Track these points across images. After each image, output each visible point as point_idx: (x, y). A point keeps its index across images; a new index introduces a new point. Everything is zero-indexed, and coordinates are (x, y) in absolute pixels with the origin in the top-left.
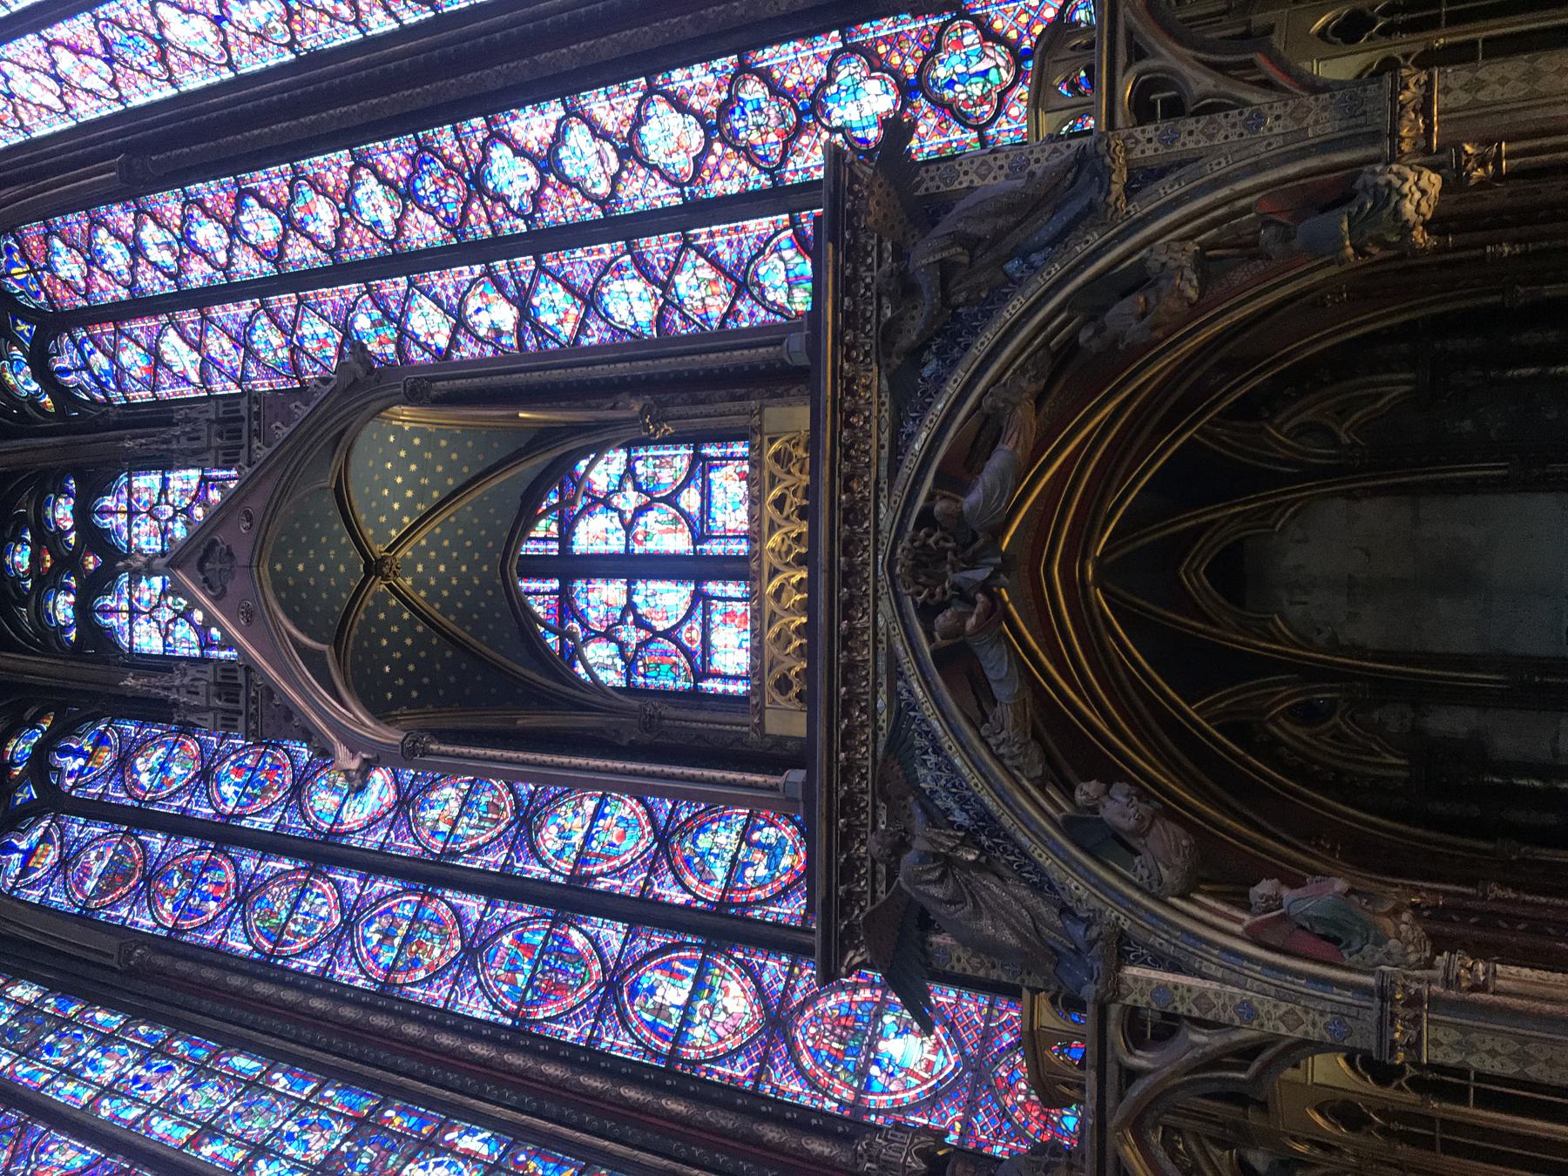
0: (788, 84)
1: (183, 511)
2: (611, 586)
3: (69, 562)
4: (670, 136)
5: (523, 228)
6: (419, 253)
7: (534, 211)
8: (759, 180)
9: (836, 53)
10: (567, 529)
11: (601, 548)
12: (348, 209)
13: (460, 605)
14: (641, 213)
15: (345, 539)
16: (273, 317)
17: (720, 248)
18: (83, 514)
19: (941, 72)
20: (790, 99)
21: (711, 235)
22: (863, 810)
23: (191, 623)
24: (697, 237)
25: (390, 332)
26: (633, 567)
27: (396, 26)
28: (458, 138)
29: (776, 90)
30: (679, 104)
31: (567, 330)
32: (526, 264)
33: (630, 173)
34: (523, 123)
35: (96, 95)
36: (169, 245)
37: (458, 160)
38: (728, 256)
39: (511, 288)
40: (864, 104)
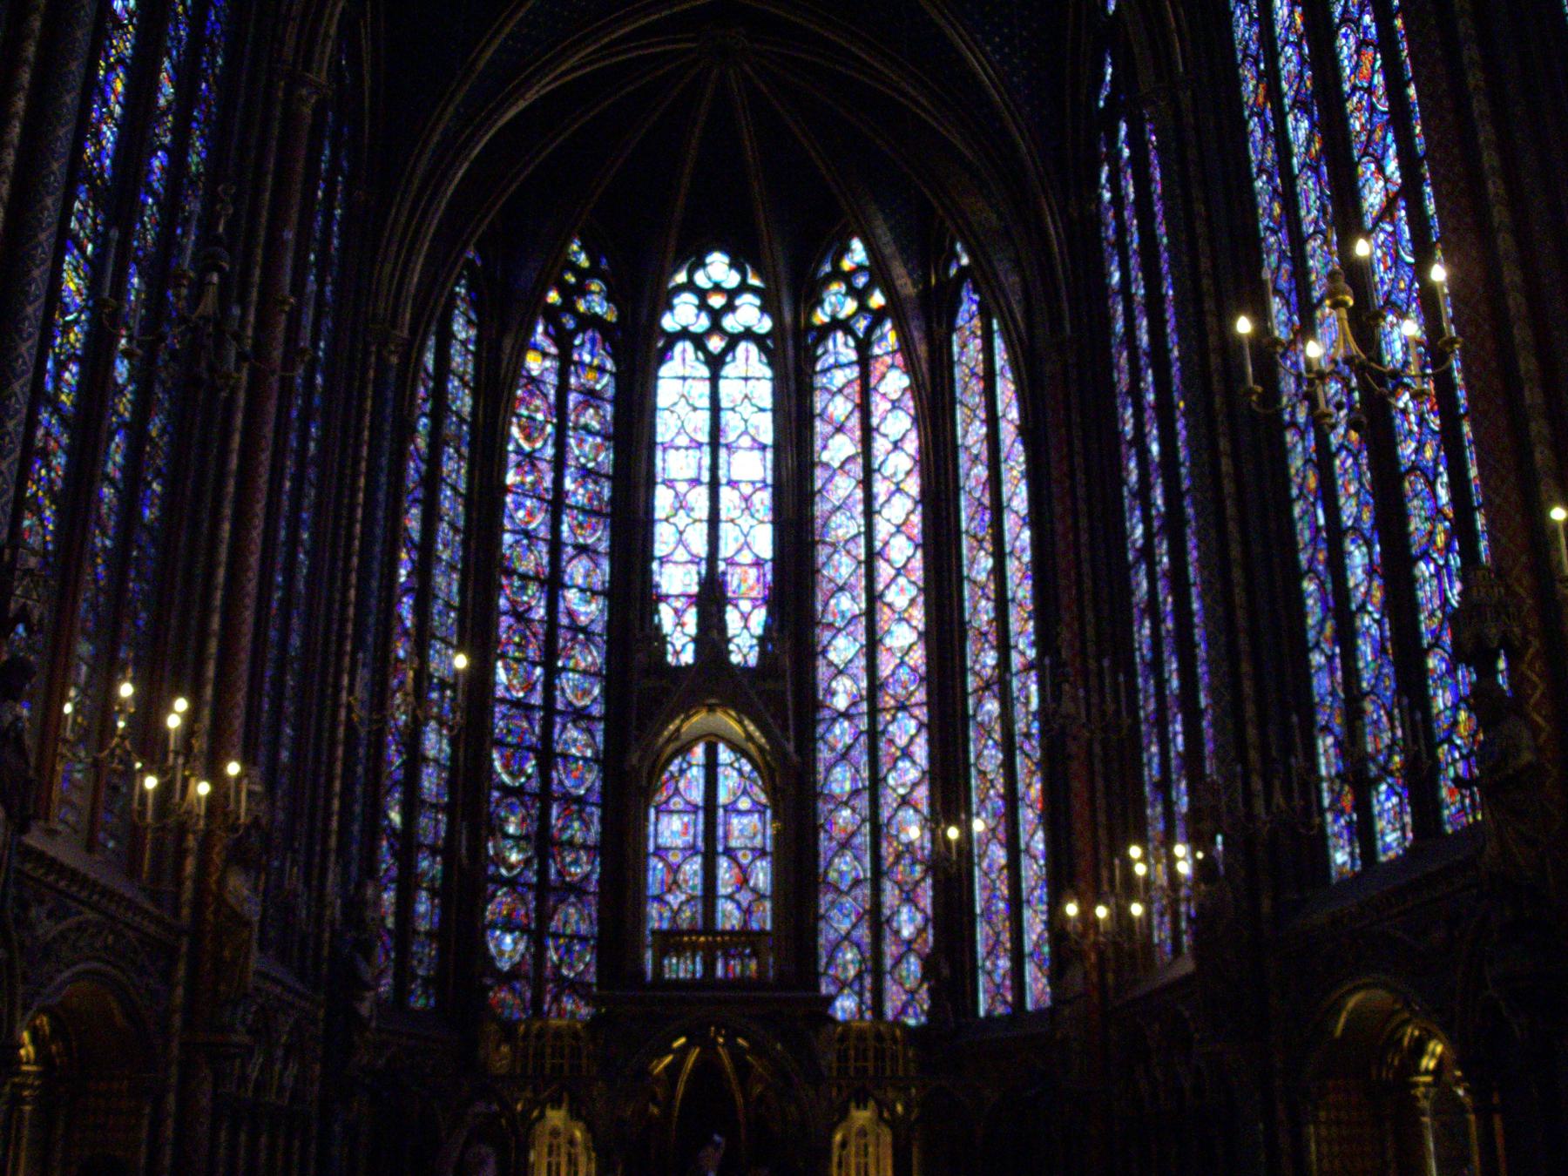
3: (716, 316)
8: (886, 865)
16: (854, 538)
18: (748, 334)
19: (912, 959)
23: (678, 433)
25: (839, 623)
26: (711, 767)
27: (970, 690)
29: (917, 883)
31: (830, 738)
32: (863, 725)
35: (968, 475)
36: (895, 474)
37: (913, 700)
38: (858, 840)
39: (853, 711)
40: (907, 923)
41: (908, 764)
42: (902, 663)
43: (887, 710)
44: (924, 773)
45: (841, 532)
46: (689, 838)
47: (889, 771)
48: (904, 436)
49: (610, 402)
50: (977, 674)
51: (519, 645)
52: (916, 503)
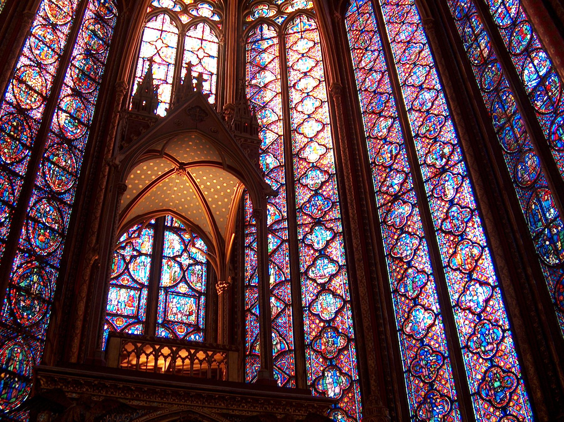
0: (342, 357)
1: (200, 62)
2: (150, 247)
4: (328, 305)
5: (299, 238)
6: (294, 192)
7: (305, 244)
8: (308, 339)
9: (351, 377)
10: (176, 231)
11: (166, 245)
12: (313, 166)
13: (159, 193)
14: (300, 289)
15: (197, 159)
17: (284, 319)
18: (205, 20)
20: (336, 356)
21: (289, 316)
22: (100, 392)
24: (289, 309)
28: (335, 219)
29: (340, 351)
30: (339, 312)
32: (285, 235)
33: (315, 287)
34: (338, 247)
35: (364, 81)
39: (276, 227)
41: (326, 261)
42: (316, 194)
43: (306, 225)
44: (340, 267)
45: (265, 120)
46: (135, 310)
47: (309, 267)
48: (311, 70)
49: (112, 28)
50: (386, 193)
51: (15, 128)
52: (322, 102)
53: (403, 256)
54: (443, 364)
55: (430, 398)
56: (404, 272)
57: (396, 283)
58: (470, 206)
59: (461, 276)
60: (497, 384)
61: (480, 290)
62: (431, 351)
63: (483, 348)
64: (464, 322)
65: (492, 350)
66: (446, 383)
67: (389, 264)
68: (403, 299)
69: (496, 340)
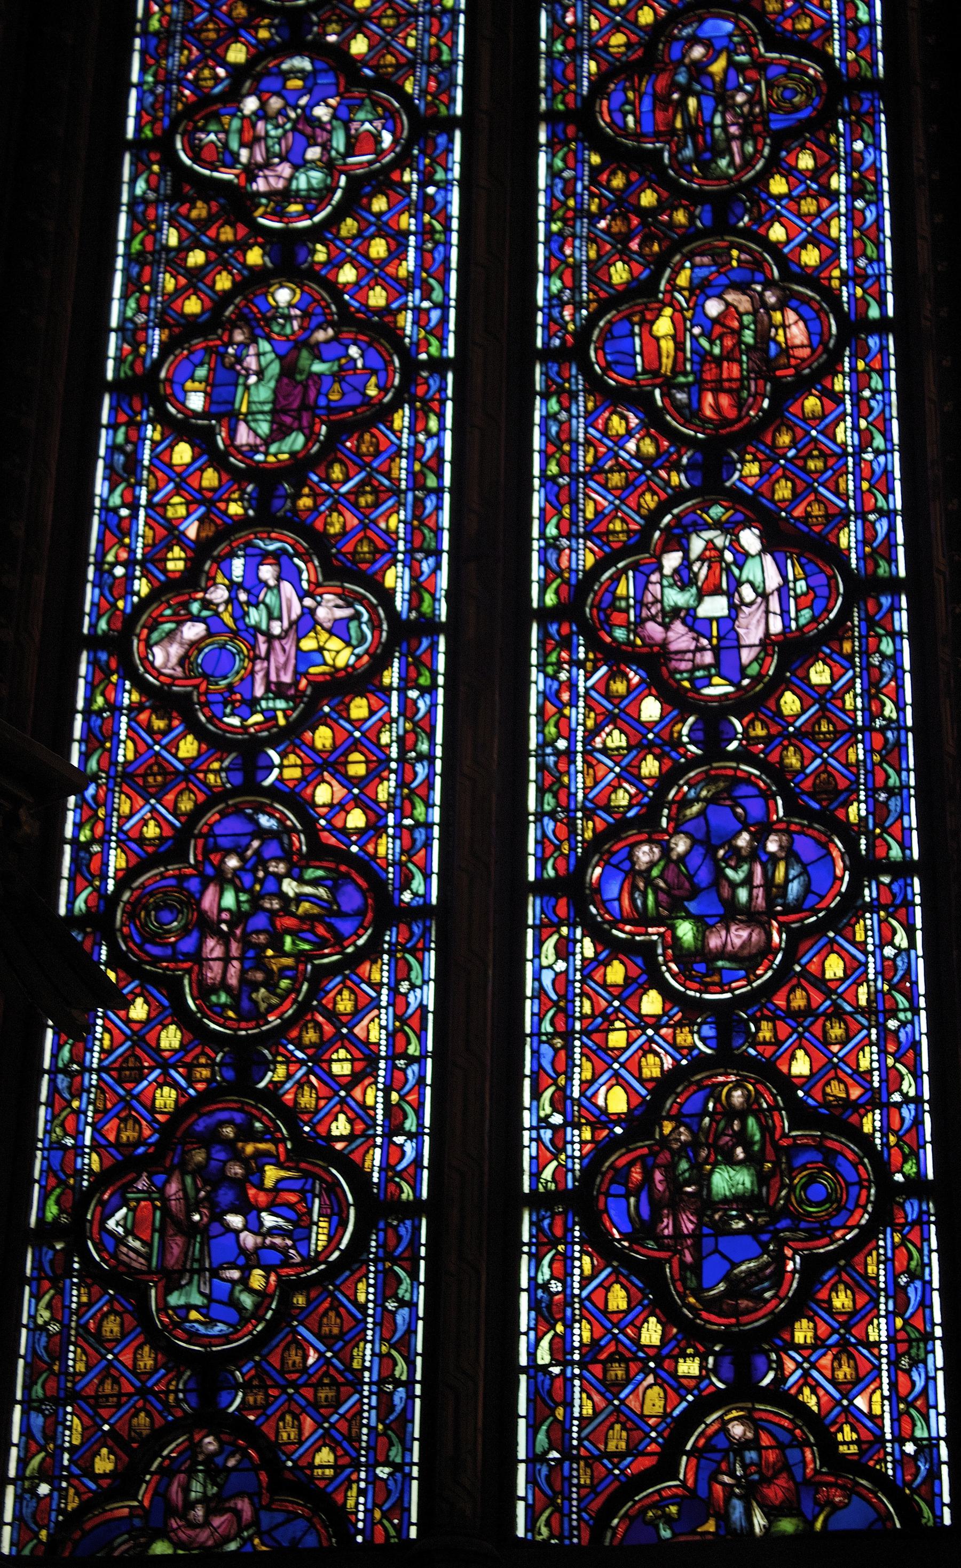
53: (260, 185)
54: (371, 952)
55: (211, 1139)
56: (238, 288)
57: (156, 336)
58: (835, 49)
59: (648, 448)
60: (727, 1181)
61: (764, 572)
62: (301, 842)
63: (686, 931)
64: (590, 735)
65: (748, 960)
66: (356, 1079)
67: (134, 201)
68: (183, 453)
69: (798, 907)
